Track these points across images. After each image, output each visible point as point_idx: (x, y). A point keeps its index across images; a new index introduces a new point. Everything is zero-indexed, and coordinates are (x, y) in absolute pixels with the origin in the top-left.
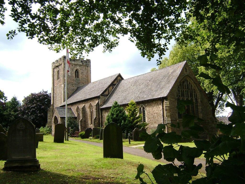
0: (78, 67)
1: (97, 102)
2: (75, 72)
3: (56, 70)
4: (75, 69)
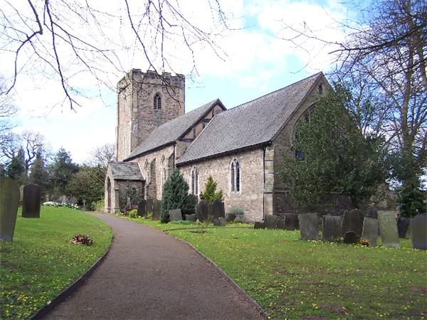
0: (160, 90)
1: (172, 152)
2: (155, 98)
3: (122, 96)
4: (154, 93)
